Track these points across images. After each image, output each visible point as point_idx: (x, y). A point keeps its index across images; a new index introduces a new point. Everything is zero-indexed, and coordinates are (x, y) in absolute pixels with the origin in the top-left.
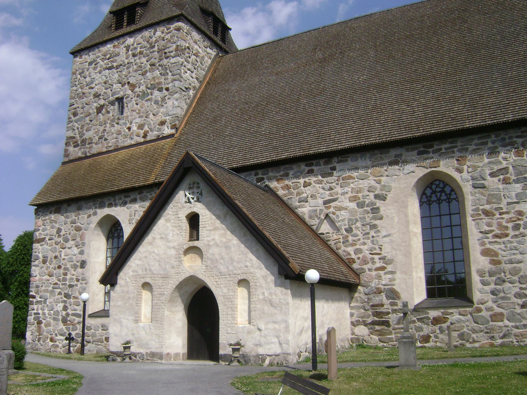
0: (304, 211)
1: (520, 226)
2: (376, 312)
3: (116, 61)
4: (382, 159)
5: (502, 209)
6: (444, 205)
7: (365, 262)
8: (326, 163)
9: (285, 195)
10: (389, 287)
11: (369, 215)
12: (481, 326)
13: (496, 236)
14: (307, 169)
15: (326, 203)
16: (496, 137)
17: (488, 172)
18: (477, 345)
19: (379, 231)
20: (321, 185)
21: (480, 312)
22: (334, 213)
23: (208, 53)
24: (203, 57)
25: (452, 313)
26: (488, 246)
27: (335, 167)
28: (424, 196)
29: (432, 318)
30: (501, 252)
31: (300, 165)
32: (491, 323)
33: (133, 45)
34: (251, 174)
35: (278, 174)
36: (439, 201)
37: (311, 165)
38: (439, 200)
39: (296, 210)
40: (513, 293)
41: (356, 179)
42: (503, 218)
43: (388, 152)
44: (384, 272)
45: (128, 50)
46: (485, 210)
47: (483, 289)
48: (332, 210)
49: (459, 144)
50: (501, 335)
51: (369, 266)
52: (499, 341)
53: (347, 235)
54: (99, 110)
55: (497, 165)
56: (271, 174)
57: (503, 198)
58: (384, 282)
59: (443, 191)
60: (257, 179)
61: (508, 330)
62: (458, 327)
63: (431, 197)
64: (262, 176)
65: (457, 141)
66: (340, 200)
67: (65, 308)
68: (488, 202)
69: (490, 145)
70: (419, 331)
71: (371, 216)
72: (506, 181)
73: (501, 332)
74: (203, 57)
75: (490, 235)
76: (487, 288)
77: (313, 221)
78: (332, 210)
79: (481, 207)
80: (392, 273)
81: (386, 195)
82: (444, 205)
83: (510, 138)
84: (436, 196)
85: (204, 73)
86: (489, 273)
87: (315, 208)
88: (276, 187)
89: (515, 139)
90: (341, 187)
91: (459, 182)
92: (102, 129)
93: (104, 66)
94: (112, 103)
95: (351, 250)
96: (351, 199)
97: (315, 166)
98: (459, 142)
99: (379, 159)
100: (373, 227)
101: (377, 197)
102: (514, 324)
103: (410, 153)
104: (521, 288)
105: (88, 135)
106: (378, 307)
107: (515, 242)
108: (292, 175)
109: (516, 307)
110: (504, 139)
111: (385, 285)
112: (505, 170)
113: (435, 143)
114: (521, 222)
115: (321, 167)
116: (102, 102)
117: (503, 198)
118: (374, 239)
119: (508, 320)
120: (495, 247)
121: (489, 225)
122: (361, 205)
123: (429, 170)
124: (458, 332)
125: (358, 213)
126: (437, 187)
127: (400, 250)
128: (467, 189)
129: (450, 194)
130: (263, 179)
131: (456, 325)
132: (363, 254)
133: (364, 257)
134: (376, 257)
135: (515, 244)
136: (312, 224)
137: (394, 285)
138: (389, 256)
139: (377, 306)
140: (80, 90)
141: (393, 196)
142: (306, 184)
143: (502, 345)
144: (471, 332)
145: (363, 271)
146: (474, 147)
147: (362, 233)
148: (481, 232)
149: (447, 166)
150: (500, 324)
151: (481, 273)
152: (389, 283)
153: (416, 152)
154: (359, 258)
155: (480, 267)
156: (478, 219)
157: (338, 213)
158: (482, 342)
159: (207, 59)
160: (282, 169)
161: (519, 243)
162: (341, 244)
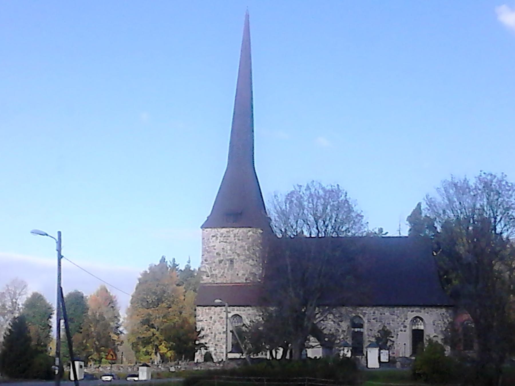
3: (228, 239)
33: (238, 234)
45: (235, 237)
54: (220, 262)
67: (215, 350)
92: (223, 271)
93: (222, 240)
94: (228, 260)
105: (214, 272)
112: (376, 318)
116: (222, 259)
140: (207, 248)
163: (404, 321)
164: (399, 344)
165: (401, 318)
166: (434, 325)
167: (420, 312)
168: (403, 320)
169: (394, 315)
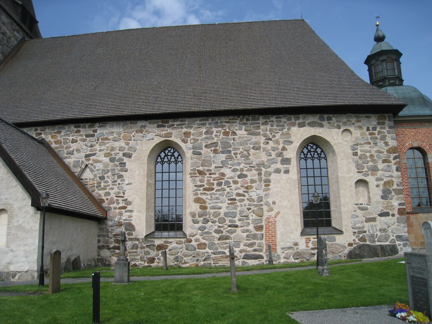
0: (70, 161)
1: (222, 184)
2: (117, 240)
4: (131, 128)
5: (211, 171)
6: (173, 165)
7: (112, 202)
8: (90, 127)
9: (57, 148)
10: (128, 221)
11: (117, 168)
12: (191, 252)
13: (205, 189)
14: (76, 129)
15: (87, 156)
16: (212, 121)
17: (204, 144)
18: (187, 265)
19: (124, 180)
20: (85, 143)
21: (190, 242)
22: (92, 165)
23: (15, 36)
24: (10, 38)
25: (171, 242)
26: (200, 196)
27: (97, 130)
28: (159, 158)
29: (156, 246)
30: (207, 201)
31: (71, 126)
32: (197, 250)
34: (31, 130)
35: (53, 131)
36: (169, 162)
37: (79, 127)
38: (169, 161)
39: (64, 160)
40: (214, 229)
41: (111, 141)
42: (211, 177)
43: (136, 123)
44: (125, 210)
46: (200, 170)
47: (193, 226)
48: (91, 162)
49: (186, 123)
50: (204, 258)
51: (115, 205)
52: (202, 263)
53: (100, 182)
55: (210, 140)
56: (47, 131)
57: (212, 163)
58: (124, 218)
59: (173, 155)
60: (36, 133)
61: (208, 255)
62: (174, 252)
63: (164, 158)
64: (40, 132)
65: (185, 120)
66: (97, 155)
68: (202, 166)
69: (207, 125)
70: (147, 255)
71: (119, 169)
72: (215, 152)
73: (203, 257)
74: (10, 38)
75: (201, 188)
76: (197, 226)
77: (76, 169)
78: (91, 162)
79: (197, 168)
80: (131, 211)
81: (132, 154)
82: (173, 165)
83: (221, 122)
84: (168, 158)
85: (9, 50)
86: (198, 215)
87: (79, 159)
88: (50, 141)
89: (224, 124)
90: (100, 145)
91: (183, 149)
95: (102, 192)
96: (106, 155)
97: (82, 128)
98: (187, 121)
99: (129, 127)
100: (120, 176)
101: (124, 155)
102: (212, 251)
103: (151, 125)
104: (219, 227)
106: (118, 236)
107: (218, 195)
108: (64, 133)
109: (215, 239)
110: (217, 123)
111: (124, 220)
112: (216, 144)
113: (170, 120)
114: (223, 181)
115: (86, 129)
117: (212, 163)
118: (120, 185)
119: (209, 248)
120: (204, 197)
121: (201, 181)
122: (112, 160)
123: (164, 139)
124: (174, 256)
125: (110, 166)
126: (169, 152)
127: (138, 195)
128: (188, 154)
129: (178, 158)
130: (41, 134)
131: (173, 251)
132: (111, 196)
133: (112, 198)
134: (120, 199)
135: (218, 196)
136: (75, 171)
137: (131, 220)
138: (129, 199)
139: (118, 235)
141: (136, 155)
142: (73, 141)
143: (203, 266)
144: (183, 256)
145: (110, 209)
146: (197, 126)
147: (111, 181)
148: (195, 186)
149: (177, 137)
150: (204, 251)
151: (193, 215)
152: (128, 219)
153: (156, 125)
154: (107, 199)
155: (192, 211)
156: (194, 177)
157: (95, 164)
158: (190, 264)
159: (14, 40)
160: (56, 128)
161: (220, 195)
162: (95, 188)
163: (284, 149)
164: (274, 203)
165: (277, 142)
166: (355, 154)
167: (322, 126)
168: (280, 147)
169: (259, 134)
